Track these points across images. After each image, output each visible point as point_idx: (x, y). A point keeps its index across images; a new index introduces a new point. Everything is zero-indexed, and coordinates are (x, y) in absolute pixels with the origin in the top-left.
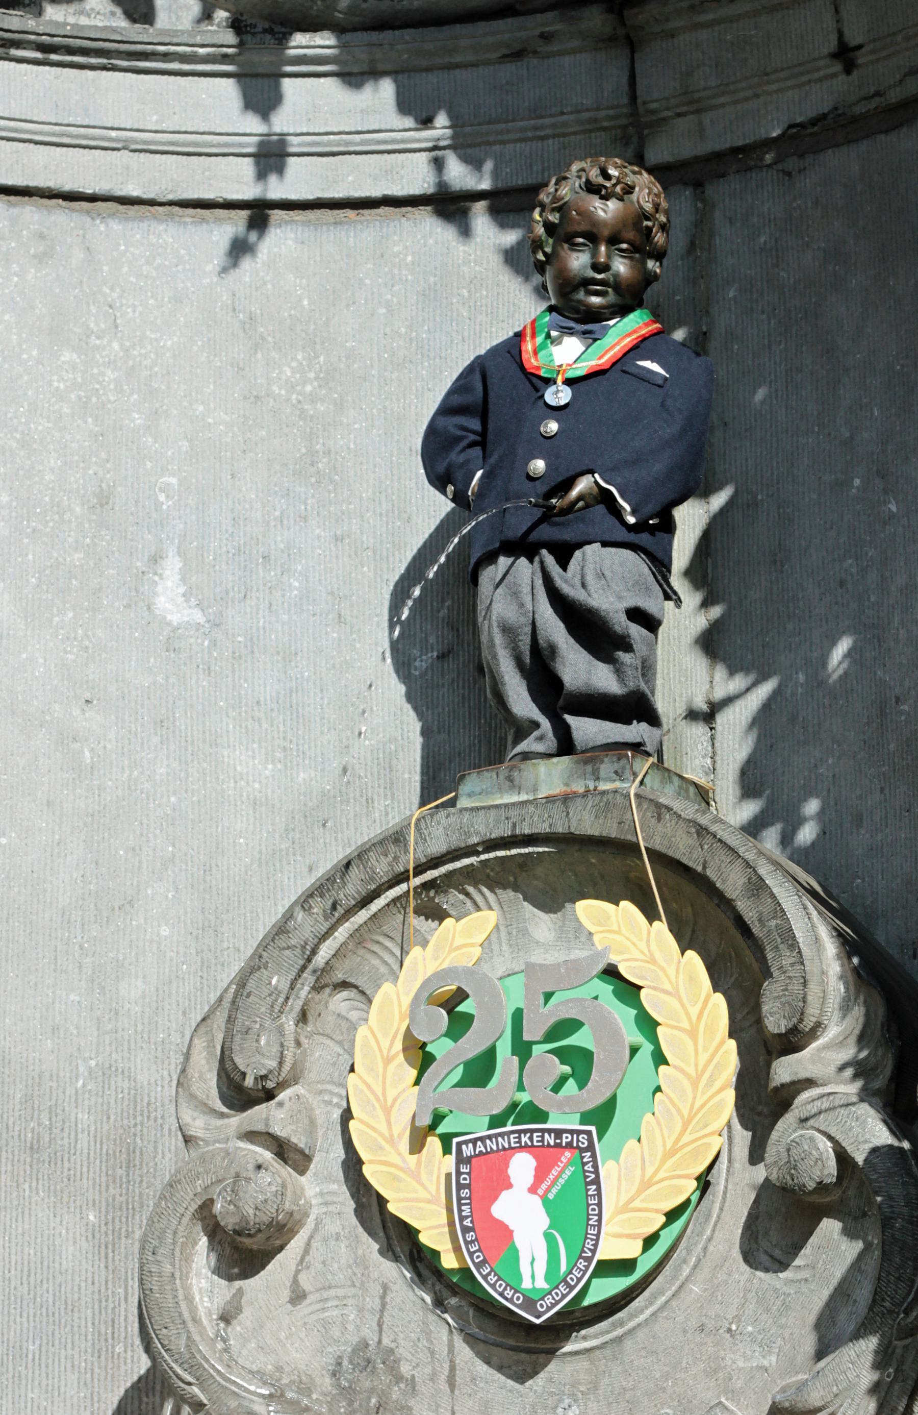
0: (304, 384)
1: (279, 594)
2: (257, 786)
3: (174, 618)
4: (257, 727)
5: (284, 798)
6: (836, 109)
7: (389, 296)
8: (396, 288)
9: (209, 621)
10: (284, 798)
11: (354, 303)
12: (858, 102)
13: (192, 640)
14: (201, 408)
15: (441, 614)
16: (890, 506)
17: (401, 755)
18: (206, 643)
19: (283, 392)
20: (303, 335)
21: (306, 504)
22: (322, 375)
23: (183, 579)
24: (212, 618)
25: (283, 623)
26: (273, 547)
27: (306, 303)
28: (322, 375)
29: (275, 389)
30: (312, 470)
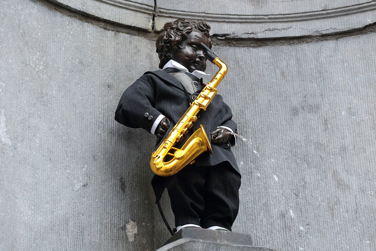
0: (40, 65)
2: (26, 217)
3: (3, 140)
6: (234, 33)
7: (65, 44)
8: (68, 42)
9: (13, 146)
11: (54, 41)
12: (244, 34)
13: (8, 151)
14: (11, 60)
15: (84, 170)
18: (12, 154)
20: (39, 47)
23: (6, 126)
24: (14, 144)
25: (34, 155)
28: (45, 64)
29: (31, 63)
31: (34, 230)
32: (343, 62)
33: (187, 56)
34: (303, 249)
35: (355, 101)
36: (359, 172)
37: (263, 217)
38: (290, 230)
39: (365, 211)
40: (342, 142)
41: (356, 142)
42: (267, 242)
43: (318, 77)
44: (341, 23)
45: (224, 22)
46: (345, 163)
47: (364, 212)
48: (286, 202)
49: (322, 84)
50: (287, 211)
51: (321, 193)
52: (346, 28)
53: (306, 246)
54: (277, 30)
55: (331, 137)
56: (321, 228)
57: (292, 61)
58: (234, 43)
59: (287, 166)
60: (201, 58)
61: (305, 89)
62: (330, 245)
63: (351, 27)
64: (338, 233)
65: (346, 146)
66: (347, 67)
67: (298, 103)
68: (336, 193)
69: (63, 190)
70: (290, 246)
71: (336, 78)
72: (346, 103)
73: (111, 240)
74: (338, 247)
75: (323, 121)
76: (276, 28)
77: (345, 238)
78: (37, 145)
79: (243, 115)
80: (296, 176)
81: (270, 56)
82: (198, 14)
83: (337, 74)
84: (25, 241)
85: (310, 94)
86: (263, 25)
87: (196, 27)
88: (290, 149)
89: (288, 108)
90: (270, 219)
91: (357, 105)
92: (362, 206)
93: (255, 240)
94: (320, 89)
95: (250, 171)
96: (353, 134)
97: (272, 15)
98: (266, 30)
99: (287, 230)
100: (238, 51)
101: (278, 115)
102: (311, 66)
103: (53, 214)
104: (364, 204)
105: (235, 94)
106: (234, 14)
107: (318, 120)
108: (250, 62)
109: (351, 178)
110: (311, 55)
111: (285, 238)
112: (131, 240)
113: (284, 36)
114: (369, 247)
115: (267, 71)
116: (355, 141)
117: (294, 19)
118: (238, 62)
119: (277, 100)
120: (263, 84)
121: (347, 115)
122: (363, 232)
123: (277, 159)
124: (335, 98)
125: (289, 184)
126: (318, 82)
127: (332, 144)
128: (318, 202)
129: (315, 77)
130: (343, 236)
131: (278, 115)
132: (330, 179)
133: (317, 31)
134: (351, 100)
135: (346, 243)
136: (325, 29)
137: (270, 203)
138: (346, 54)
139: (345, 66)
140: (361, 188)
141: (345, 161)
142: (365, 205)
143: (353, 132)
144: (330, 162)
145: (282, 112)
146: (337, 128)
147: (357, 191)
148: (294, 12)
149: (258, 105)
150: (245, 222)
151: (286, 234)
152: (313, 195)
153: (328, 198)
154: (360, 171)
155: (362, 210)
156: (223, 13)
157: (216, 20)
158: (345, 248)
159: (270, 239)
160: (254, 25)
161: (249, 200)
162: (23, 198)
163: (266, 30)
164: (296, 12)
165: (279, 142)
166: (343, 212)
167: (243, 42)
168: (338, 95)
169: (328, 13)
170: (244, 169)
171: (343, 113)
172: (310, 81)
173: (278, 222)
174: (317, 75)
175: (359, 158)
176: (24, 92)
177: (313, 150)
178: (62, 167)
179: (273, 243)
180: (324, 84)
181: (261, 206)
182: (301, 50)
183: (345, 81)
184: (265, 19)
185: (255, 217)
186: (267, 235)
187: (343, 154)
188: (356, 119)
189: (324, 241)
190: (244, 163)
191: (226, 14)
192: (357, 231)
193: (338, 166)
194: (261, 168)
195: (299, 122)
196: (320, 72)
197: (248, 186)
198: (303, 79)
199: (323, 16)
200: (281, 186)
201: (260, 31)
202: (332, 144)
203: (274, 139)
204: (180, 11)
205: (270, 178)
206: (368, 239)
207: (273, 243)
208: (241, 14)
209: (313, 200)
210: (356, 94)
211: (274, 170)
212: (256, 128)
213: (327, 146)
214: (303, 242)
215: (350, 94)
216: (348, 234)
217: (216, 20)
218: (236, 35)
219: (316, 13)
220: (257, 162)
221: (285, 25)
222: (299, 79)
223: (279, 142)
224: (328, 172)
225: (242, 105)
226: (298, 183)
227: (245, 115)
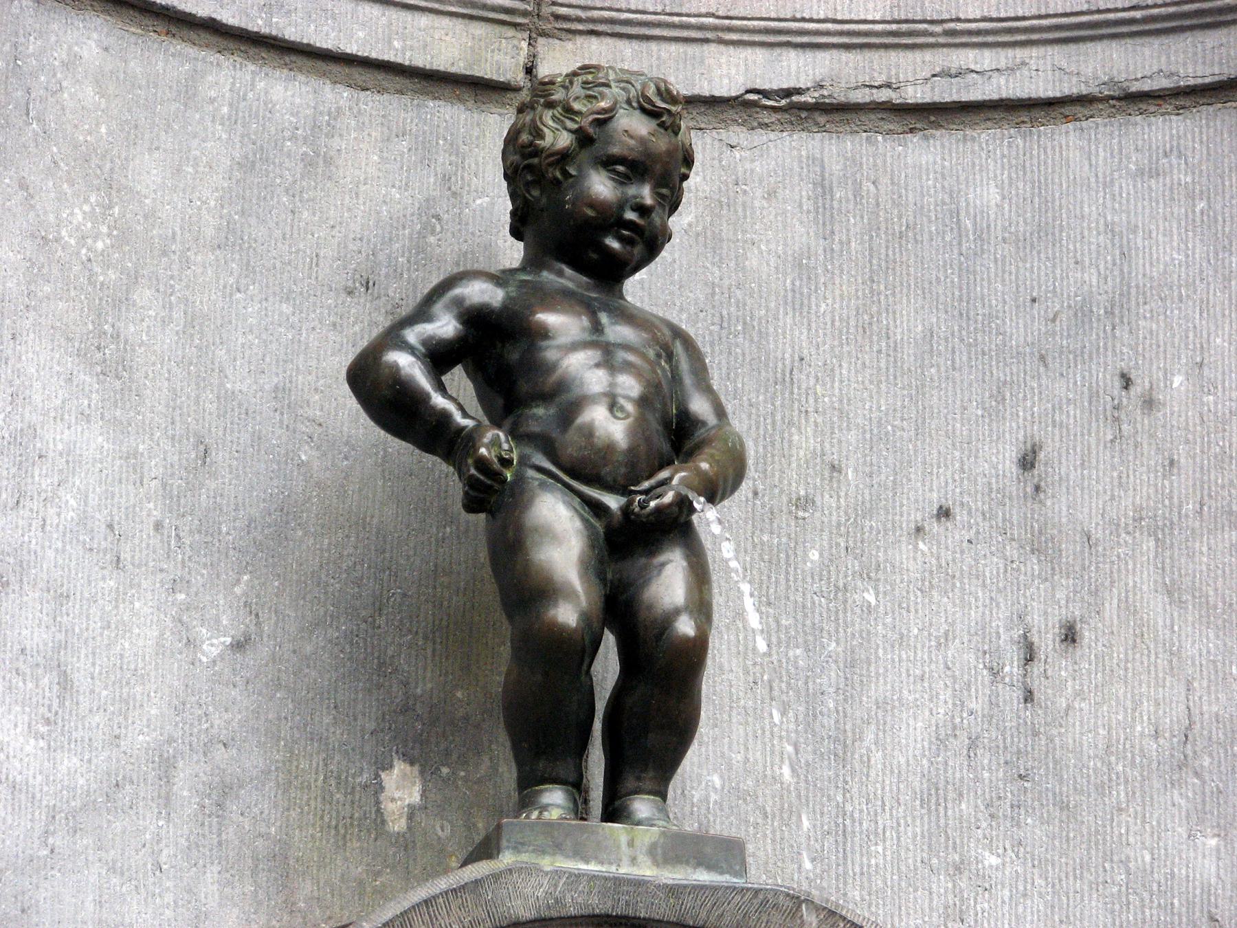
0: (96, 238)
1: (56, 510)
2: (18, 765)
4: (21, 684)
5: (45, 789)
6: (822, 87)
8: (209, 145)
10: (45, 789)
11: (157, 149)
15: (238, 590)
16: (866, 595)
17: (180, 764)
19: (73, 242)
20: (99, 172)
21: (90, 399)
22: (115, 233)
25: (57, 550)
26: (51, 446)
27: (103, 130)
29: (64, 233)
30: (99, 355)
31: (45, 803)
32: (1191, 196)
33: (594, 204)
34: (1000, 861)
35: (1218, 341)
36: (1208, 596)
37: (873, 747)
38: (961, 795)
39: (1214, 736)
40: (1163, 486)
41: (1209, 488)
42: (876, 834)
43: (1106, 248)
44: (1195, 54)
45: (788, 44)
46: (1168, 561)
47: (1210, 738)
48: (955, 696)
49: (1116, 273)
50: (954, 728)
51: (1076, 667)
52: (1208, 71)
53: (1009, 851)
54: (974, 75)
55: (1128, 469)
56: (1065, 789)
57: (1021, 185)
58: (822, 119)
59: (971, 567)
60: (643, 210)
61: (1058, 290)
62: (1088, 850)
63: (1226, 71)
64: (1120, 810)
65: (1176, 500)
66: (1202, 213)
67: (1029, 339)
68: (1126, 669)
69: (157, 664)
70: (954, 848)
71: (1165, 252)
72: (1187, 344)
73: (322, 828)
74: (1115, 858)
75: (1108, 407)
76: (972, 67)
77: (1139, 826)
78: (71, 514)
79: (833, 381)
80: (998, 606)
81: (943, 167)
82: (693, 20)
83: (1167, 239)
84: (8, 843)
85: (1071, 312)
86: (928, 55)
87: (629, 102)
88: (986, 507)
89: (991, 357)
90: (896, 753)
91: (1223, 354)
92: (1206, 716)
93: (837, 825)
94: (1106, 292)
95: (841, 584)
96: (1202, 460)
97: (958, 20)
98: (934, 76)
99: (951, 795)
100: (834, 148)
101: (954, 383)
102: (1082, 208)
103: (118, 746)
104: (1215, 709)
105: (810, 308)
106: (822, 16)
107: (1090, 403)
108: (872, 188)
109: (1180, 615)
110: (1087, 167)
111: (942, 821)
112: (398, 825)
113: (995, 97)
114: (1214, 859)
115: (930, 222)
116: (1206, 487)
117: (1035, 37)
118: (831, 188)
119: (956, 328)
120: (912, 269)
121: (1188, 391)
122: (1199, 807)
123: (939, 543)
124: (1154, 326)
125: (972, 631)
126: (1102, 267)
127: (1131, 493)
128: (1063, 700)
129: (1093, 247)
130: (1136, 818)
131: (954, 383)
132: (1111, 618)
133: (1111, 80)
134: (1205, 336)
135: (1143, 843)
136: (1139, 76)
137: (900, 699)
138: (1204, 167)
139: (1198, 209)
140: (1208, 652)
141: (1168, 553)
142: (1217, 715)
143: (1202, 452)
144: (1119, 557)
145: (970, 373)
146: (1151, 436)
147: (1193, 664)
148: (1034, 12)
149: (888, 346)
150: (808, 764)
151: (946, 807)
152: (1049, 673)
153: (1096, 686)
154: (1211, 593)
155: (1205, 733)
156: (782, 16)
157: (757, 38)
158: (1136, 861)
159: (888, 823)
160: (893, 54)
161: (830, 685)
162: (8, 700)
163: (934, 76)
164: (1043, 12)
165: (950, 481)
166: (1142, 734)
167: (848, 116)
168: (1166, 316)
169: (1153, 19)
170: (821, 575)
171: (1177, 380)
172: (1077, 263)
173: (922, 766)
174: (1101, 238)
175: (1213, 547)
176: (32, 336)
177: (1064, 513)
178: (158, 585)
179: (898, 838)
180: (1121, 270)
181: (869, 710)
182: (1053, 148)
183: (1194, 264)
184: (932, 34)
185: (845, 746)
186: (879, 811)
187: (1163, 530)
188: (1216, 403)
189: (1071, 835)
190: (821, 555)
191: (794, 20)
192: (1183, 802)
193: (1142, 572)
194: (881, 575)
195: (1024, 411)
196: (1112, 231)
197: (830, 639)
198: (1054, 253)
199: (1134, 28)
200: (942, 640)
201: (914, 76)
202: (1131, 493)
203: (935, 471)
204: (629, 11)
205: (908, 611)
206: (1216, 831)
207: (898, 838)
208: (847, 17)
209: (1050, 691)
210: (1224, 315)
211: (923, 580)
212: (875, 431)
213: (1112, 498)
214: (1001, 837)
215: (1205, 315)
216: (1151, 817)
217: (757, 38)
218: (826, 93)
219: (1111, 16)
220: (866, 555)
221: (1004, 57)
222: (1039, 253)
223: (950, 481)
224: (1107, 594)
225: (832, 348)
226: (1001, 630)
227: (842, 382)
